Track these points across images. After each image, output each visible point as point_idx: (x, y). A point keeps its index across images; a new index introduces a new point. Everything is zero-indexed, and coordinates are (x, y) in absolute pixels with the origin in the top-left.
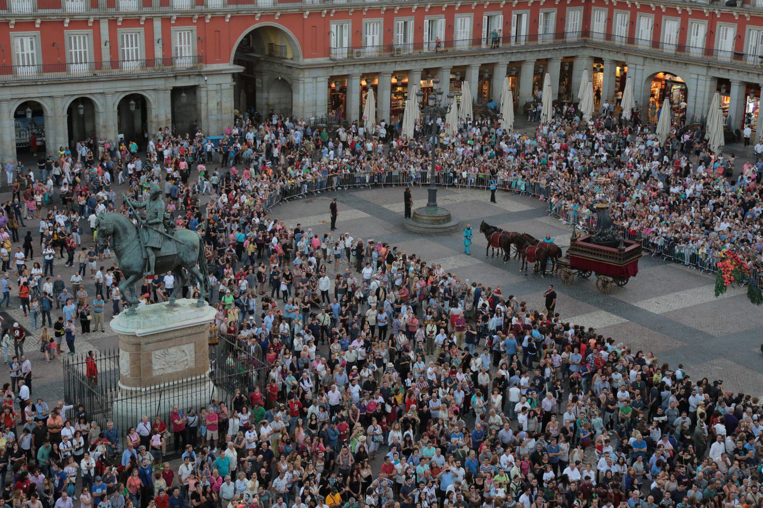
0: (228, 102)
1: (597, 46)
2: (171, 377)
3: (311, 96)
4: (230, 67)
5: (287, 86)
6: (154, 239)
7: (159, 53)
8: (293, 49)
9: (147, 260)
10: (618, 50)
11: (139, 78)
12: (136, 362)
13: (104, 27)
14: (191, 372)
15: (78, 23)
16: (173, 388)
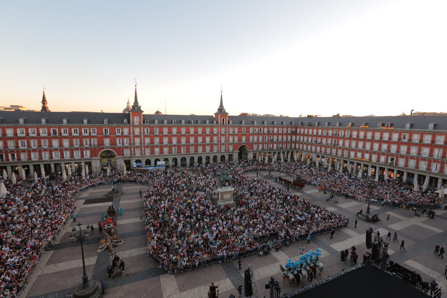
0: (237, 157)
1: (297, 149)
2: (226, 199)
3: (250, 156)
4: (238, 151)
5: (247, 154)
6: (225, 177)
7: (227, 149)
8: (248, 149)
9: (224, 180)
10: (301, 150)
11: (224, 153)
12: (221, 196)
13: (219, 145)
14: (230, 198)
15: (216, 144)
16: (227, 201)
